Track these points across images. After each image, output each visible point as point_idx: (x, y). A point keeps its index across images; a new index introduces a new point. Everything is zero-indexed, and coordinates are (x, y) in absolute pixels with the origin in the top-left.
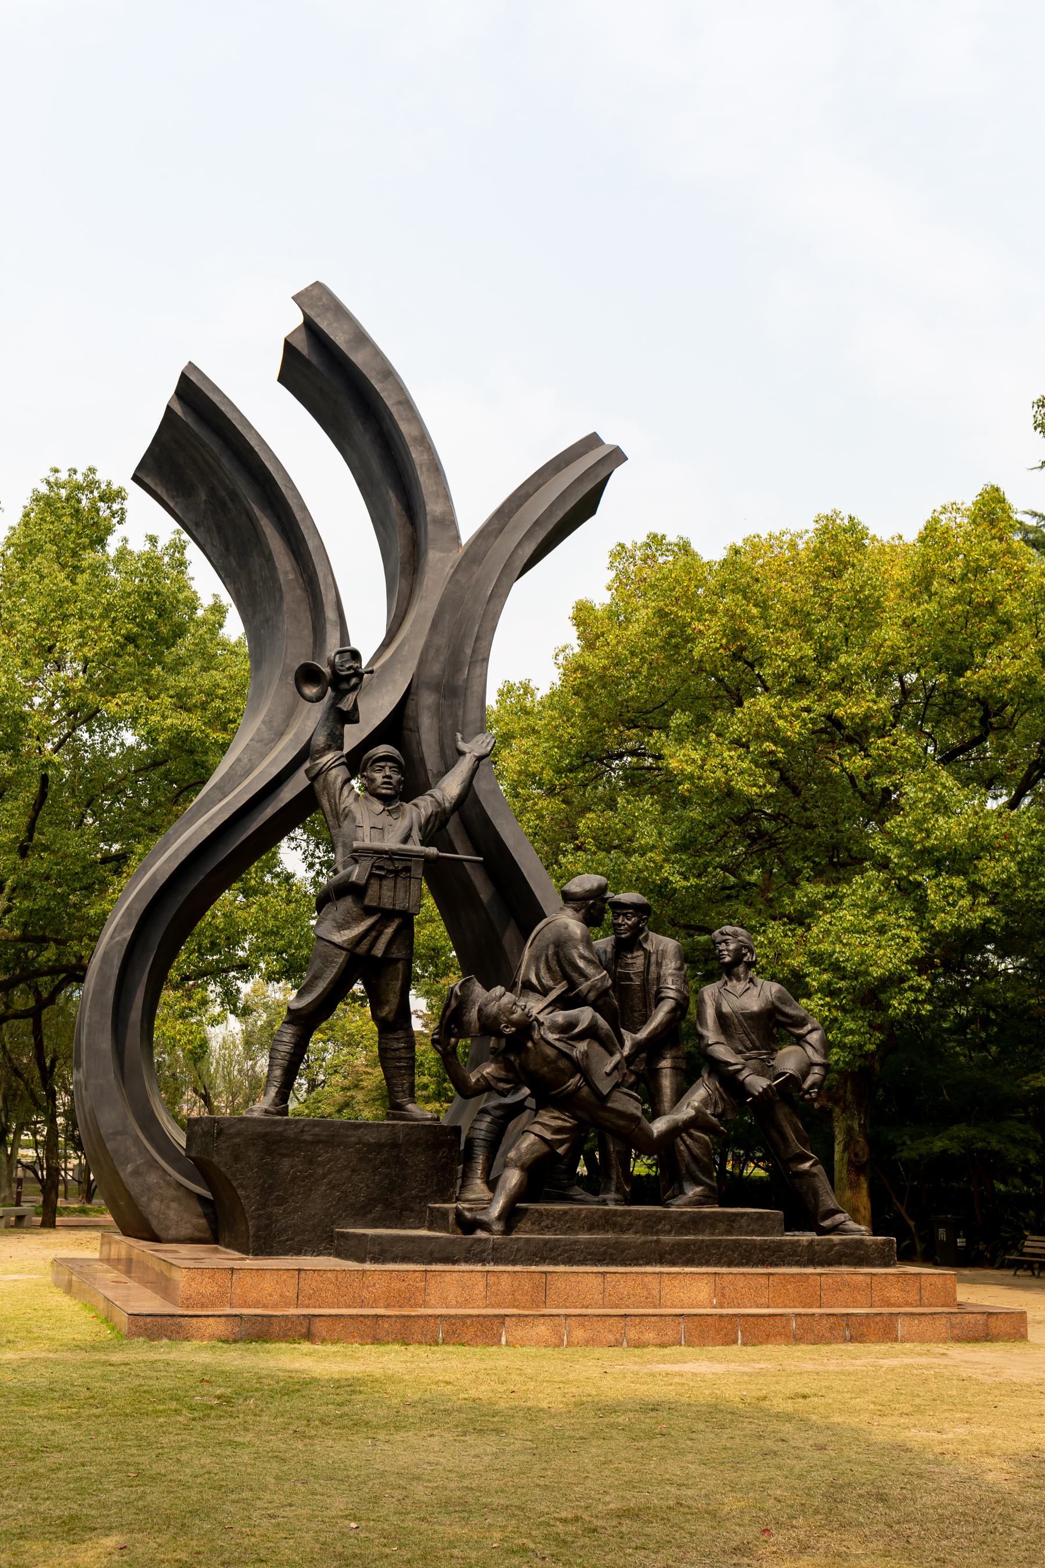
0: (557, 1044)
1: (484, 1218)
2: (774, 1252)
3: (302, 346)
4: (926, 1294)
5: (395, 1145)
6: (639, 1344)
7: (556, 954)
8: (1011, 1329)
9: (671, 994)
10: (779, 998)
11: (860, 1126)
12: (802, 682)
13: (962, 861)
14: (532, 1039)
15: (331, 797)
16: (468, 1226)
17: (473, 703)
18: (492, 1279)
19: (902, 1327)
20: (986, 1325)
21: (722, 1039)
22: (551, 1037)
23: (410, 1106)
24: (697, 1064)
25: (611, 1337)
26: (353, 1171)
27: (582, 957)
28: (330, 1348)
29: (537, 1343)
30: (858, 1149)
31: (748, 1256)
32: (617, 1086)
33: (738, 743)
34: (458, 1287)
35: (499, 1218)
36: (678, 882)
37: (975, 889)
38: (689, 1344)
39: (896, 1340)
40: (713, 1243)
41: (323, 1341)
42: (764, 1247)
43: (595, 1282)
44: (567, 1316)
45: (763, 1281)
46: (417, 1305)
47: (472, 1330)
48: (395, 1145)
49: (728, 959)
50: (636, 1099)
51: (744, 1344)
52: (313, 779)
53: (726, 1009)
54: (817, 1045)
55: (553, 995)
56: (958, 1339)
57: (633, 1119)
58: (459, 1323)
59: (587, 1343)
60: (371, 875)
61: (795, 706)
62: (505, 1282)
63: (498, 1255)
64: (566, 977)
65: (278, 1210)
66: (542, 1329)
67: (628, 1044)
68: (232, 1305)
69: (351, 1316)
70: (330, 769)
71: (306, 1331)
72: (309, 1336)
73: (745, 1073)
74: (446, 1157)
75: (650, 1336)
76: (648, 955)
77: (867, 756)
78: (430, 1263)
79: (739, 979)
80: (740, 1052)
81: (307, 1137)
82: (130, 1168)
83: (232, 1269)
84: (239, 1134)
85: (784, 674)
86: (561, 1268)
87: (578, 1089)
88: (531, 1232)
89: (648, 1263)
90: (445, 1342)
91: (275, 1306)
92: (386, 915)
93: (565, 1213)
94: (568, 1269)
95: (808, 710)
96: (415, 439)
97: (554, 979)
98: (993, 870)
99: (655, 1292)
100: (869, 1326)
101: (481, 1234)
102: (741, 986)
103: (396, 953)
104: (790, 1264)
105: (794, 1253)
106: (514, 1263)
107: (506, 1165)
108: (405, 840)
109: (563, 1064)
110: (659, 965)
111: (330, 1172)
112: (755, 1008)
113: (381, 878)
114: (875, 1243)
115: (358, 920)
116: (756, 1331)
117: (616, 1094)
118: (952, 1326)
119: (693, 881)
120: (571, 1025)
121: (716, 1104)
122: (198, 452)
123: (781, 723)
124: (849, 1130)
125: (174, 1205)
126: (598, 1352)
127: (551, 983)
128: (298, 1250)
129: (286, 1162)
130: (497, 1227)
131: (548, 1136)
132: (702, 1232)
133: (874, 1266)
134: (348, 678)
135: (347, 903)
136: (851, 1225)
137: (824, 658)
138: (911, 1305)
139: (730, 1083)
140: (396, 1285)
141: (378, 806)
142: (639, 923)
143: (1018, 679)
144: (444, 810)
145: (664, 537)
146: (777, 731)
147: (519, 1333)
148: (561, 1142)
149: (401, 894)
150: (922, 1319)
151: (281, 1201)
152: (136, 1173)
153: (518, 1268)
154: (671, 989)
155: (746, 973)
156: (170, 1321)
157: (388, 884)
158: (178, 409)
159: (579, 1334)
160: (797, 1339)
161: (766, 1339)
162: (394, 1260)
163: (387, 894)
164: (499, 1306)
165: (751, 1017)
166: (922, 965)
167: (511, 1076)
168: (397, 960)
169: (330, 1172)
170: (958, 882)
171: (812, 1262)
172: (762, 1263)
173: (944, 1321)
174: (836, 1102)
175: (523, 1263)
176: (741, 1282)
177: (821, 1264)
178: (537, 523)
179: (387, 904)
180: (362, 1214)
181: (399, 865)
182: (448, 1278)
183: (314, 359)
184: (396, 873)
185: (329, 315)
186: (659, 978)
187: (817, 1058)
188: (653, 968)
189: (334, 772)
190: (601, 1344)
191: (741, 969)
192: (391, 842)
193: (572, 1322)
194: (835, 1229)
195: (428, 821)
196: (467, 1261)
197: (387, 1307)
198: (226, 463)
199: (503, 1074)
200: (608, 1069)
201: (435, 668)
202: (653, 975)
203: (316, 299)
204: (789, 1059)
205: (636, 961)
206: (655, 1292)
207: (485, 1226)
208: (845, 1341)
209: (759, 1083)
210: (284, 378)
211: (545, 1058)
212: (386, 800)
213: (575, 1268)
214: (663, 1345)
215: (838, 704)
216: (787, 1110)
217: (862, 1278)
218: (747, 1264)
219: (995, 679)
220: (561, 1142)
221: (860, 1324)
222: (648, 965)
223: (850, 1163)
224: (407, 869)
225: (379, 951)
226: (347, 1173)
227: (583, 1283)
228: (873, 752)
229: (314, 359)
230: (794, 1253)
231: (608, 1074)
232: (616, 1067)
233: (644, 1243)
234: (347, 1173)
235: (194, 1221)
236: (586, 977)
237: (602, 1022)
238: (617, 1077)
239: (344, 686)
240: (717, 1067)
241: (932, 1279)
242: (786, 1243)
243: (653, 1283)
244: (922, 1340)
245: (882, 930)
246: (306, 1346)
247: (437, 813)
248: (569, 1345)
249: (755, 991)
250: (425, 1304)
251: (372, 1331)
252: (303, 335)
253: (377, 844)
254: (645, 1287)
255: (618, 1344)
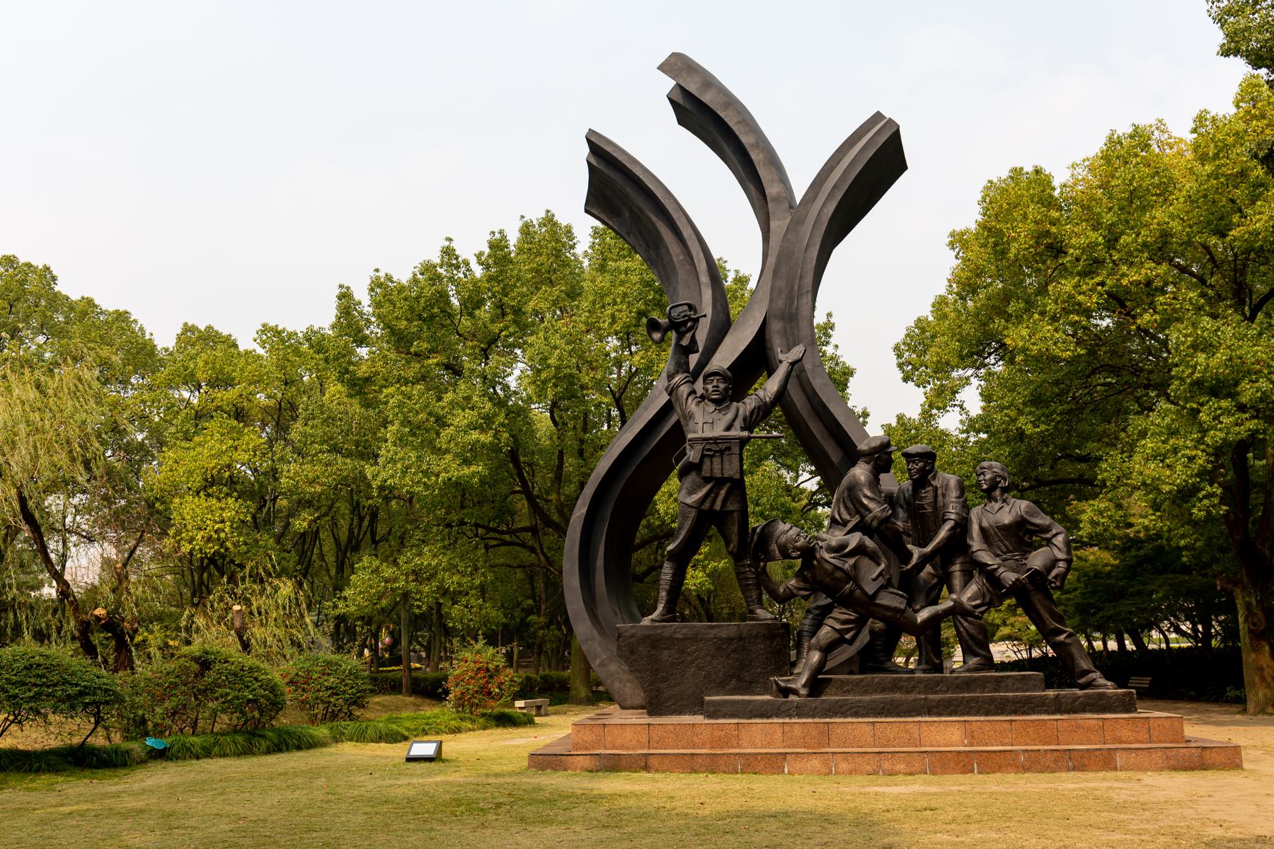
0: (832, 561)
1: (793, 686)
2: (1025, 704)
3: (680, 99)
4: (1155, 734)
5: (741, 638)
6: (892, 773)
7: (849, 496)
8: (1230, 759)
9: (953, 516)
10: (1027, 513)
11: (1257, 601)
12: (1098, 262)
13: (1229, 386)
14: (815, 558)
15: (681, 405)
16: (786, 692)
17: (803, 324)
18: (787, 728)
19: (1120, 759)
20: (1201, 757)
21: (985, 546)
22: (827, 556)
23: (759, 611)
24: (974, 567)
25: (869, 768)
26: (713, 657)
27: (866, 497)
28: (657, 776)
29: (812, 772)
30: (1255, 620)
31: (1002, 707)
32: (882, 588)
33: (1054, 319)
34: (760, 735)
35: (804, 686)
36: (1029, 429)
37: (1242, 408)
38: (933, 773)
39: (1115, 769)
40: (972, 699)
41: (657, 771)
42: (1015, 701)
43: (869, 728)
44: (834, 753)
45: (1007, 726)
46: (732, 747)
47: (762, 764)
48: (741, 638)
49: (985, 487)
50: (901, 596)
51: (980, 772)
52: (670, 394)
53: (985, 524)
54: (1061, 545)
55: (850, 526)
56: (1175, 768)
57: (896, 610)
58: (752, 759)
59: (850, 773)
60: (703, 456)
61: (1091, 282)
62: (797, 731)
63: (800, 711)
64: (858, 512)
65: (664, 686)
66: (815, 763)
67: (915, 557)
68: (605, 748)
69: (674, 754)
70: (678, 386)
71: (644, 764)
72: (646, 768)
73: (1001, 570)
74: (780, 646)
75: (901, 767)
76: (936, 489)
77: (1155, 312)
78: (750, 718)
79: (996, 501)
80: (998, 556)
81: (678, 636)
82: (597, 662)
83: (694, 725)
84: (633, 636)
85: (1078, 260)
86: (837, 720)
87: (852, 592)
88: (836, 694)
89: (919, 714)
90: (742, 772)
91: (634, 748)
92: (719, 482)
93: (862, 680)
94: (855, 720)
95: (1102, 284)
96: (752, 146)
97: (850, 514)
98: (1248, 392)
99: (916, 736)
100: (1089, 759)
101: (792, 697)
102: (997, 506)
103: (731, 507)
104: (1039, 713)
105: (1043, 704)
106: (813, 716)
107: (810, 649)
108: (728, 428)
109: (838, 574)
110: (944, 495)
111: (696, 658)
112: (1007, 522)
113: (711, 457)
114: (1116, 694)
115: (700, 487)
116: (990, 763)
117: (883, 594)
118: (1167, 757)
119: (1043, 427)
120: (842, 547)
121: (984, 596)
122: (616, 185)
123: (1080, 298)
124: (1248, 606)
125: (628, 684)
126: (859, 778)
127: (847, 517)
128: (680, 712)
129: (666, 653)
130: (803, 692)
131: (838, 626)
132: (974, 691)
133: (1116, 712)
134: (685, 323)
135: (692, 477)
136: (1102, 681)
137: (1112, 242)
138: (1142, 742)
139: (991, 577)
140: (718, 733)
141: (712, 407)
142: (925, 467)
143: (1266, 230)
144: (765, 403)
145: (1021, 169)
146: (1080, 304)
147: (798, 765)
148: (848, 630)
149: (727, 466)
150: (1139, 752)
151: (665, 680)
152: (602, 665)
153: (817, 720)
154: (953, 512)
155: (1002, 495)
156: (554, 758)
157: (717, 460)
158: (594, 162)
159: (844, 766)
160: (1025, 769)
161: (1000, 768)
162: (724, 716)
163: (717, 467)
164: (794, 747)
165: (1004, 528)
166: (1208, 475)
167: (807, 586)
168: (732, 512)
169: (696, 658)
170: (1224, 403)
171: (1058, 710)
172: (1015, 712)
173: (1160, 754)
174: (1235, 583)
175: (820, 717)
176: (987, 727)
177: (1067, 712)
178: (835, 187)
179: (717, 474)
180: (721, 687)
181: (723, 447)
182: (754, 728)
183: (687, 106)
184: (722, 452)
185: (684, 74)
186: (944, 505)
187: (1061, 555)
188: (940, 498)
189: (682, 388)
190: (861, 773)
191: (998, 492)
192: (718, 431)
193: (838, 757)
194: (1089, 685)
195: (752, 413)
196: (778, 716)
197: (712, 748)
198: (630, 190)
199: (802, 585)
200: (874, 576)
201: (780, 303)
202: (940, 503)
203: (677, 65)
204: (1037, 560)
205: (927, 494)
206: (916, 736)
207: (795, 692)
208: (1069, 770)
209: (1010, 577)
210: (681, 122)
211: (826, 570)
212: (717, 402)
213: (860, 720)
214: (911, 774)
215: (1123, 275)
216: (1040, 596)
217: (1094, 722)
218: (1002, 713)
219: (1251, 233)
220: (848, 630)
221: (1082, 757)
222: (936, 496)
223: (1250, 631)
224: (729, 449)
225: (718, 507)
226: (709, 658)
227: (858, 731)
228: (1159, 308)
229: (687, 106)
230: (1043, 704)
231: (874, 580)
232: (880, 574)
233: (915, 700)
234: (709, 658)
235: (639, 697)
236: (869, 511)
237: (869, 542)
238: (881, 581)
239: (683, 329)
240: (982, 567)
241: (1160, 722)
242: (1035, 697)
243: (914, 730)
244: (1140, 768)
245: (1175, 450)
246: (645, 774)
247: (759, 407)
248: (837, 773)
249: (1007, 508)
250: (739, 746)
251: (690, 764)
252: (678, 91)
253: (708, 434)
254: (907, 732)
255: (875, 773)
